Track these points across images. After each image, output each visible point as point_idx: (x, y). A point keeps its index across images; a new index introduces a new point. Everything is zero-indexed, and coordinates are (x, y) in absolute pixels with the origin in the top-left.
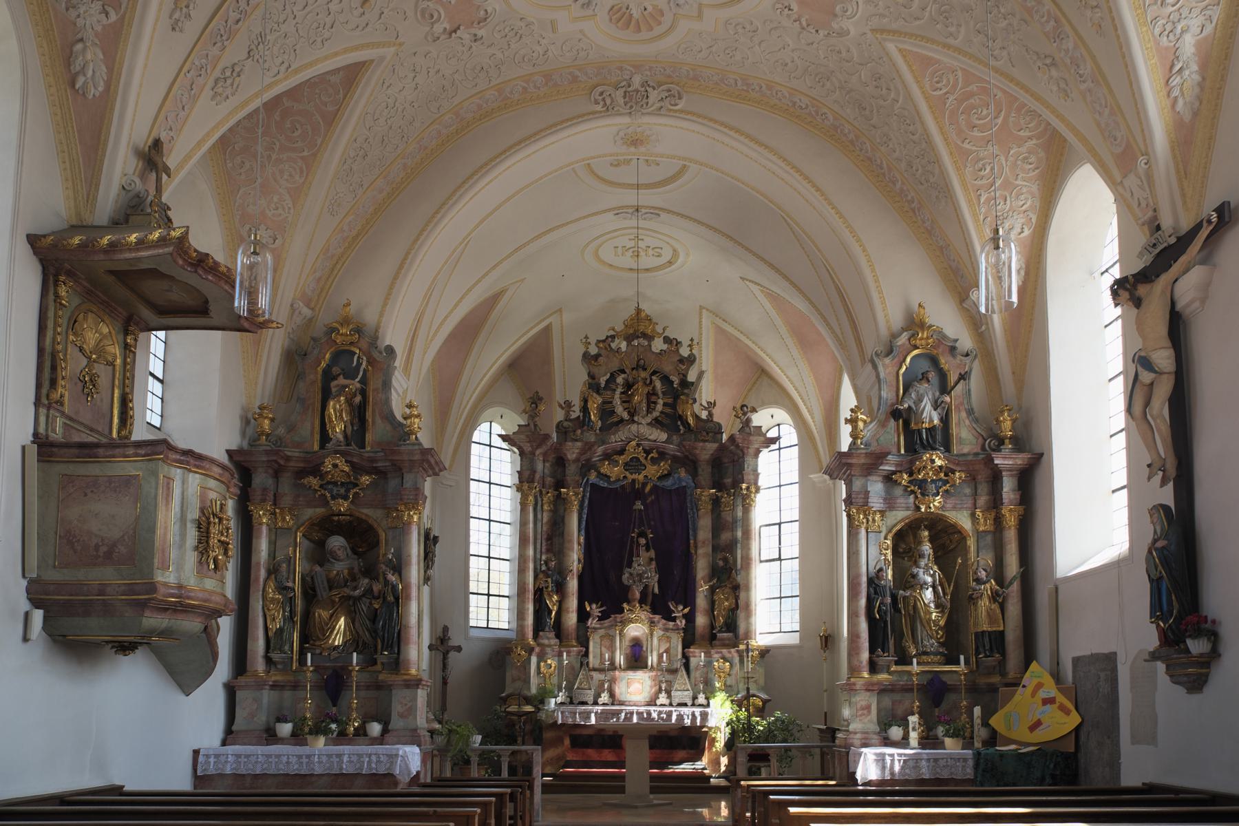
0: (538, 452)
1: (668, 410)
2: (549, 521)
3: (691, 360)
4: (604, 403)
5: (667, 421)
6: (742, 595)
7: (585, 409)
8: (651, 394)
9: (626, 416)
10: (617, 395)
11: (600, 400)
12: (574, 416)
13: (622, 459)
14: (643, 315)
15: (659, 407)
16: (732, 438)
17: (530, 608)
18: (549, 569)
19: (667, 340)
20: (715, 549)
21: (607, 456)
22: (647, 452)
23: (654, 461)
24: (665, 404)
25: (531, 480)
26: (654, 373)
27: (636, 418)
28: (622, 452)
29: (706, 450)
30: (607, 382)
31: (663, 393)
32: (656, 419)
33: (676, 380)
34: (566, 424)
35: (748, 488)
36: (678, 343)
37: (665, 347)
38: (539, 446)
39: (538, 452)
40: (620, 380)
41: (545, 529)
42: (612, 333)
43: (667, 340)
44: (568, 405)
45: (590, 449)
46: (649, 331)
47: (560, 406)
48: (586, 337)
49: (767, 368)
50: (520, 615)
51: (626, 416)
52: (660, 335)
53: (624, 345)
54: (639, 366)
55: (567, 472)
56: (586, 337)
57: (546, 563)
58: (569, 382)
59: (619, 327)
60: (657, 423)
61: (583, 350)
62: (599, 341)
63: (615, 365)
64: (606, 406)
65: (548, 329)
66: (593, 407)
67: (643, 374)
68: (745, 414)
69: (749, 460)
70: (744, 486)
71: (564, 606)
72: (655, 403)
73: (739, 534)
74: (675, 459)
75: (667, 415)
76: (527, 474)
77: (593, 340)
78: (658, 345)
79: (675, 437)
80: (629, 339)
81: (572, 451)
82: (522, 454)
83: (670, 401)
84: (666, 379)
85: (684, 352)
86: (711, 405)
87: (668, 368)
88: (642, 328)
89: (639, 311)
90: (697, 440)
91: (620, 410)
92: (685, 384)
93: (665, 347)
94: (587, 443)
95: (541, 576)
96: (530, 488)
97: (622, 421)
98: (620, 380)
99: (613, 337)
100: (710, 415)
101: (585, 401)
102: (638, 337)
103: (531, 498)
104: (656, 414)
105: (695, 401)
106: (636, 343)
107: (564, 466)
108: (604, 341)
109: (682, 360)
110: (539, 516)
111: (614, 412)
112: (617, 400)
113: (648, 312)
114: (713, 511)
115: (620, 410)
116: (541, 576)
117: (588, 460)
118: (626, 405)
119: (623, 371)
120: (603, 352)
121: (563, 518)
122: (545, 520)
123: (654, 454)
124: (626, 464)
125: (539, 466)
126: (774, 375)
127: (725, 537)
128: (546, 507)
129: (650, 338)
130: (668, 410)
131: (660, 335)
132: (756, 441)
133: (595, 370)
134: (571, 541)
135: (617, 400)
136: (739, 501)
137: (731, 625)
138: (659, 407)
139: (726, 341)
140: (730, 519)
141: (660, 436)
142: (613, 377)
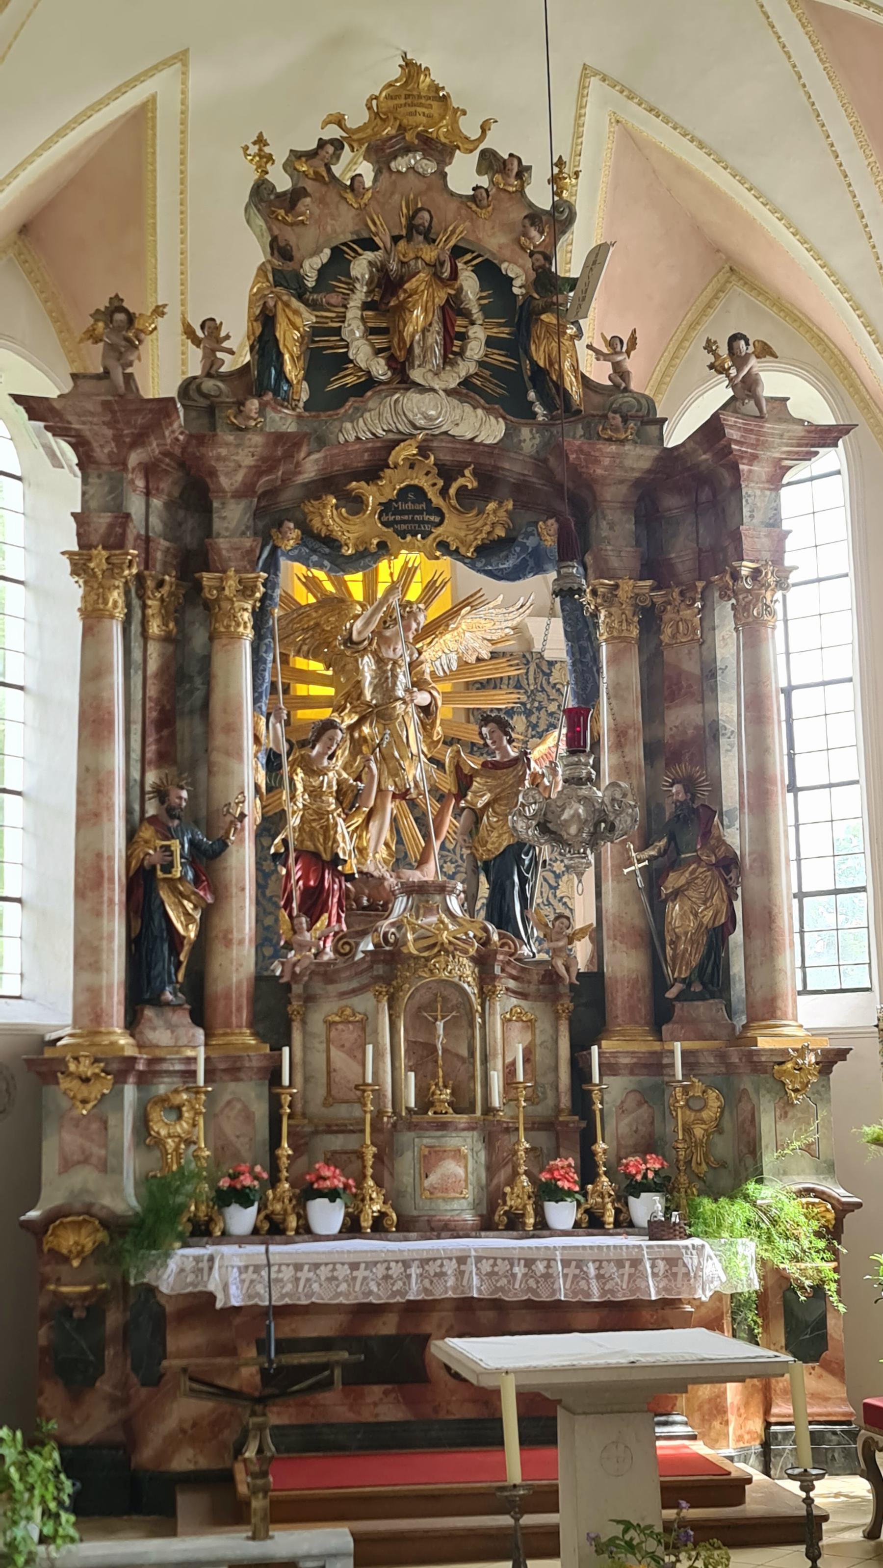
0: (134, 458)
1: (498, 358)
2: (163, 670)
3: (560, 218)
4: (317, 331)
5: (495, 389)
6: (752, 881)
7: (265, 344)
8: (452, 310)
9: (380, 369)
10: (354, 313)
11: (308, 318)
12: (228, 364)
13: (373, 496)
14: (424, 82)
15: (476, 349)
16: (712, 431)
17: (116, 929)
18: (171, 812)
19: (490, 162)
20: (652, 751)
21: (329, 484)
22: (447, 473)
23: (468, 500)
24: (491, 342)
25: (115, 541)
26: (458, 252)
27: (416, 375)
28: (372, 472)
29: (621, 462)
30: (322, 271)
31: (483, 308)
32: (466, 383)
33: (518, 273)
34: (209, 385)
35: (756, 573)
36: (523, 172)
37: (484, 181)
38: (139, 440)
39: (134, 458)
40: (361, 267)
41: (152, 691)
42: (334, 132)
43: (490, 162)
44: (210, 335)
45: (289, 455)
46: (441, 132)
47: (189, 332)
48: (260, 141)
49: (756, 257)
50: (87, 956)
51: (380, 369)
52: (470, 145)
53: (366, 170)
54: (416, 229)
55: (217, 525)
56: (260, 141)
57: (161, 794)
58: (206, 278)
59: (357, 118)
60: (466, 391)
61: (254, 176)
62: (296, 155)
63: (343, 225)
64: (323, 341)
65: (141, 118)
66: (290, 339)
67: (430, 254)
68: (739, 361)
69: (753, 495)
70: (746, 568)
71: (219, 924)
72: (463, 337)
73: (729, 708)
74: (521, 491)
75: (497, 371)
76: (103, 521)
77: (280, 153)
78: (463, 175)
79: (525, 432)
80: (381, 153)
81: (234, 460)
82: (86, 463)
83: (504, 333)
84: (490, 273)
85: (540, 195)
86: (616, 348)
87: (494, 241)
88: (419, 120)
89: (412, 70)
90: (591, 435)
91: (361, 352)
92: (547, 281)
93: (484, 181)
94: (279, 438)
95: (147, 833)
96: (113, 568)
97: (369, 383)
98: (361, 267)
99: (338, 145)
100: (620, 372)
101: (266, 320)
102: (408, 150)
103: (116, 596)
104: (466, 368)
105: (579, 334)
106: (401, 164)
107: (207, 510)
108: (310, 155)
109: (535, 217)
110: (137, 655)
111: (345, 359)
112: (354, 329)
113: (437, 76)
114: (642, 642)
115: (361, 352)
116: (147, 833)
117: (271, 493)
118: (380, 341)
119: (369, 245)
120: (310, 185)
121: (206, 662)
122: (153, 666)
123: (468, 480)
124: (386, 508)
125: (135, 505)
126: (779, 277)
127: (681, 717)
128: (155, 628)
129: (440, 151)
130: (498, 358)
131: (470, 145)
132: (777, 440)
133: (290, 236)
134: (233, 729)
135: (354, 329)
136: (724, 614)
137: (712, 976)
138: (476, 349)
139: (645, 171)
140: (691, 666)
141: (490, 430)
142: (339, 261)
